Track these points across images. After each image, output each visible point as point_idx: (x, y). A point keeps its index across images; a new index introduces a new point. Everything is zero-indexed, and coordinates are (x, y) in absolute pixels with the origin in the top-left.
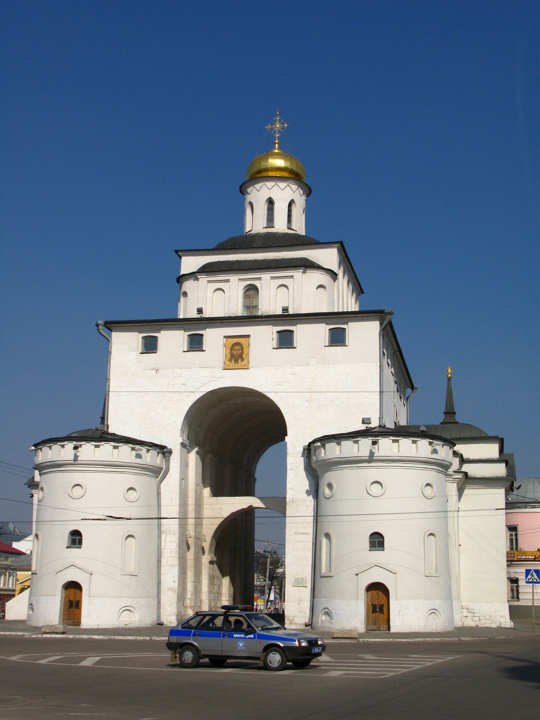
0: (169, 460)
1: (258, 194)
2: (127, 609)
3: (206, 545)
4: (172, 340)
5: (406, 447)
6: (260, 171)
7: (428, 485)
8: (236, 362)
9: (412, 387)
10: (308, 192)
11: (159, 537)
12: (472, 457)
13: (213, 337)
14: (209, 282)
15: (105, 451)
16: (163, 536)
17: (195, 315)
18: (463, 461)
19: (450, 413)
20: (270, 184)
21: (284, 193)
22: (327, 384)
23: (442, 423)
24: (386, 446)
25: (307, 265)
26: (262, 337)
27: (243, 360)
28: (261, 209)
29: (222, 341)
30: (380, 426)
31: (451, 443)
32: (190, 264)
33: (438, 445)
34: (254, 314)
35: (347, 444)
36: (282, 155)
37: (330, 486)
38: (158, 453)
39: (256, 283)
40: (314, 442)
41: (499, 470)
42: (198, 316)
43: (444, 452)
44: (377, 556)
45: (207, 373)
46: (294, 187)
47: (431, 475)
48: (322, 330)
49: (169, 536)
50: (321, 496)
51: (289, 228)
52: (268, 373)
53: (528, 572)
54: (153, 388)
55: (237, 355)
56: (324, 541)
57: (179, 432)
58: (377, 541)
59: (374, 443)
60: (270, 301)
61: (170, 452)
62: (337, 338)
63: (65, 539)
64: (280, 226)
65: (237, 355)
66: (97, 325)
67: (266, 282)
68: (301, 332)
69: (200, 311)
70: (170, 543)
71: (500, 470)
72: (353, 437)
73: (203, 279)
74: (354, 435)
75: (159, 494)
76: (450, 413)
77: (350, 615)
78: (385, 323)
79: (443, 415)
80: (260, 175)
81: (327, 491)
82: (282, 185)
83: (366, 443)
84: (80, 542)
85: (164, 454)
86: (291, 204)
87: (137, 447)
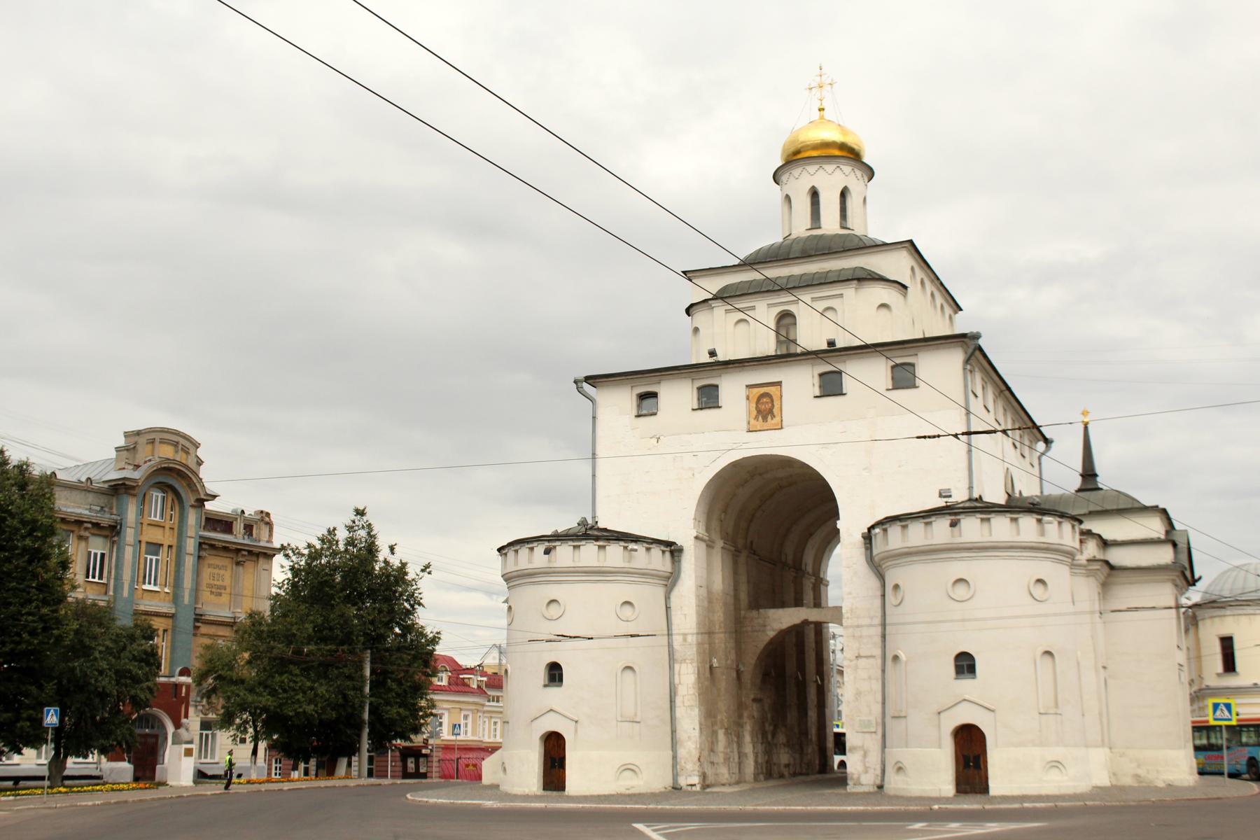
0: (680, 561)
2: (629, 768)
3: (747, 678)
4: (677, 398)
7: (1039, 581)
8: (765, 419)
9: (1047, 441)
11: (671, 668)
12: (1119, 536)
13: (733, 389)
14: (727, 311)
16: (677, 666)
17: (706, 359)
18: (1105, 544)
19: (1089, 474)
20: (812, 168)
23: (1079, 490)
26: (798, 384)
27: (773, 416)
28: (802, 204)
29: (743, 392)
30: (970, 500)
31: (1078, 520)
33: (1051, 523)
34: (792, 351)
35: (916, 529)
38: (663, 552)
39: (792, 308)
40: (873, 527)
41: (1165, 555)
42: (711, 360)
44: (966, 684)
45: (725, 437)
46: (847, 169)
49: (684, 666)
51: (843, 227)
52: (810, 433)
53: (1216, 706)
55: (765, 408)
57: (691, 523)
58: (965, 665)
59: (953, 524)
60: (812, 332)
61: (681, 550)
62: (904, 378)
63: (541, 675)
64: (830, 224)
65: (765, 408)
66: (576, 382)
69: (712, 353)
70: (688, 677)
71: (1165, 555)
72: (923, 517)
73: (719, 309)
74: (927, 515)
75: (668, 608)
76: (1089, 474)
78: (970, 351)
79: (1080, 479)
80: (799, 156)
82: (830, 168)
83: (941, 526)
84: (561, 680)
85: (672, 552)
86: (844, 194)
87: (632, 546)
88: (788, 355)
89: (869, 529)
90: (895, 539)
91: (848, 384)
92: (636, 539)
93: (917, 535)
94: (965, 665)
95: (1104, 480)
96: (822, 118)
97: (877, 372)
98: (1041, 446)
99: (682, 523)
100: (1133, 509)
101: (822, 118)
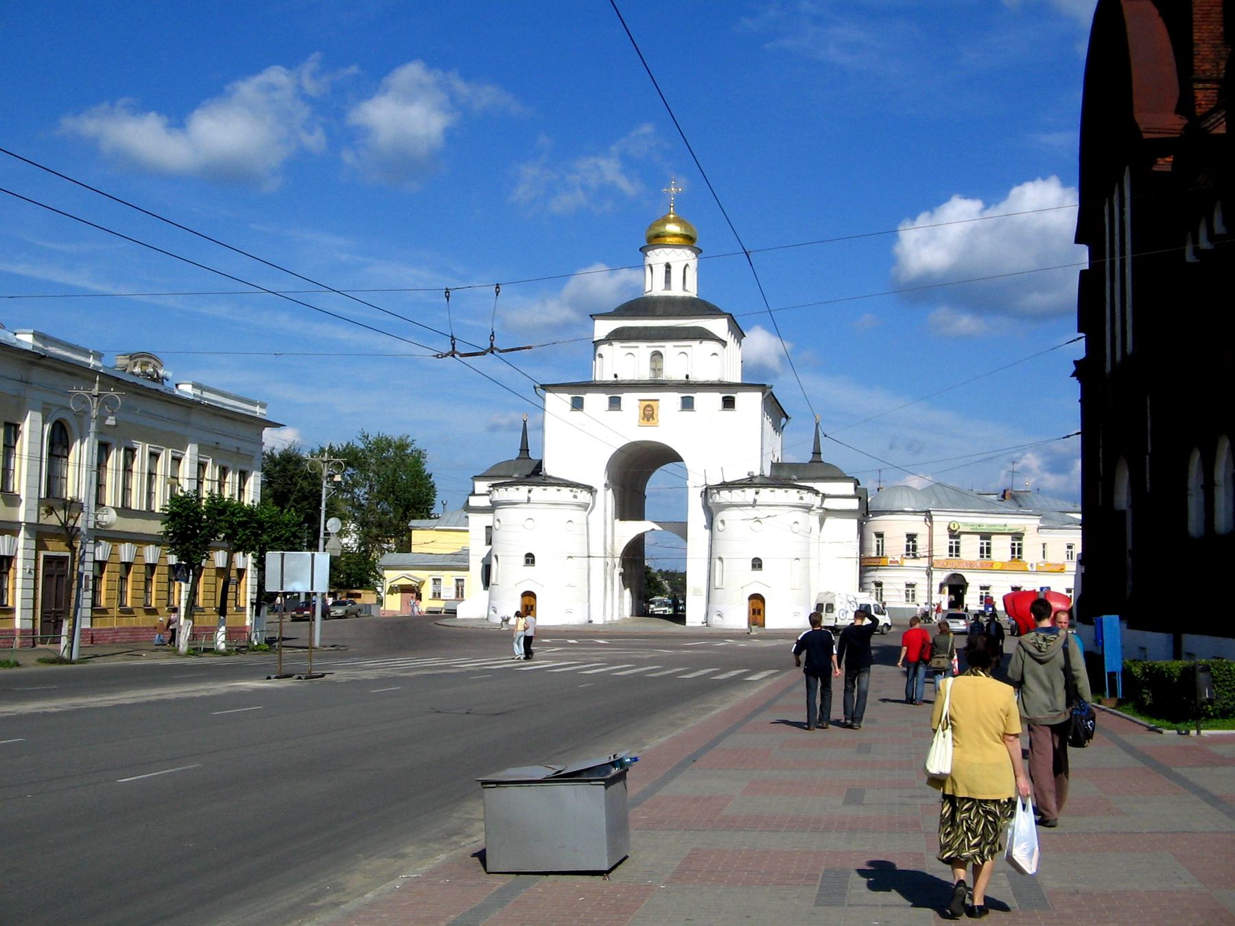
1: (658, 257)
4: (596, 401)
5: (780, 495)
6: (658, 236)
9: (787, 417)
10: (698, 252)
13: (630, 400)
15: (551, 493)
18: (825, 496)
19: (817, 453)
21: (682, 258)
22: (720, 442)
24: (766, 495)
25: (703, 335)
26: (669, 401)
28: (660, 272)
32: (603, 328)
36: (677, 221)
37: (723, 522)
41: (854, 504)
43: (809, 498)
46: (689, 252)
47: (799, 515)
48: (717, 398)
50: (715, 529)
51: (684, 289)
54: (580, 440)
55: (649, 414)
56: (718, 562)
63: (523, 560)
64: (676, 291)
65: (649, 414)
67: (669, 349)
68: (700, 398)
73: (617, 345)
76: (817, 453)
77: (736, 618)
81: (721, 526)
84: (533, 562)
90: (725, 496)
92: (577, 486)
93: (737, 496)
94: (757, 564)
95: (823, 458)
97: (717, 398)
98: (784, 420)
99: (598, 477)
100: (840, 477)
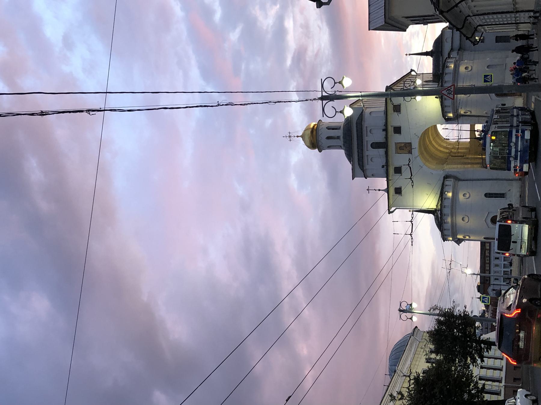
19: (426, 54)
20: (320, 138)
64: (340, 133)
66: (389, 213)
73: (367, 167)
76: (426, 54)
88: (383, 145)
89: (445, 119)
91: (397, 124)
96: (301, 136)
101: (301, 136)
